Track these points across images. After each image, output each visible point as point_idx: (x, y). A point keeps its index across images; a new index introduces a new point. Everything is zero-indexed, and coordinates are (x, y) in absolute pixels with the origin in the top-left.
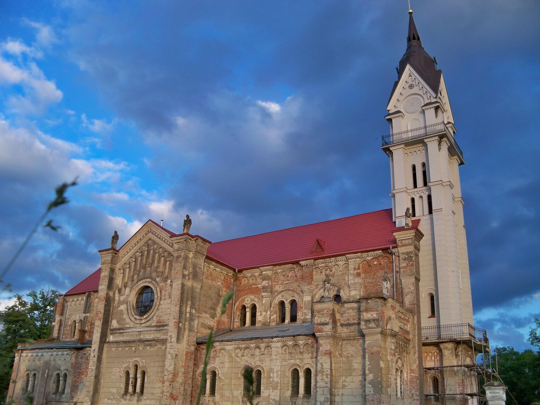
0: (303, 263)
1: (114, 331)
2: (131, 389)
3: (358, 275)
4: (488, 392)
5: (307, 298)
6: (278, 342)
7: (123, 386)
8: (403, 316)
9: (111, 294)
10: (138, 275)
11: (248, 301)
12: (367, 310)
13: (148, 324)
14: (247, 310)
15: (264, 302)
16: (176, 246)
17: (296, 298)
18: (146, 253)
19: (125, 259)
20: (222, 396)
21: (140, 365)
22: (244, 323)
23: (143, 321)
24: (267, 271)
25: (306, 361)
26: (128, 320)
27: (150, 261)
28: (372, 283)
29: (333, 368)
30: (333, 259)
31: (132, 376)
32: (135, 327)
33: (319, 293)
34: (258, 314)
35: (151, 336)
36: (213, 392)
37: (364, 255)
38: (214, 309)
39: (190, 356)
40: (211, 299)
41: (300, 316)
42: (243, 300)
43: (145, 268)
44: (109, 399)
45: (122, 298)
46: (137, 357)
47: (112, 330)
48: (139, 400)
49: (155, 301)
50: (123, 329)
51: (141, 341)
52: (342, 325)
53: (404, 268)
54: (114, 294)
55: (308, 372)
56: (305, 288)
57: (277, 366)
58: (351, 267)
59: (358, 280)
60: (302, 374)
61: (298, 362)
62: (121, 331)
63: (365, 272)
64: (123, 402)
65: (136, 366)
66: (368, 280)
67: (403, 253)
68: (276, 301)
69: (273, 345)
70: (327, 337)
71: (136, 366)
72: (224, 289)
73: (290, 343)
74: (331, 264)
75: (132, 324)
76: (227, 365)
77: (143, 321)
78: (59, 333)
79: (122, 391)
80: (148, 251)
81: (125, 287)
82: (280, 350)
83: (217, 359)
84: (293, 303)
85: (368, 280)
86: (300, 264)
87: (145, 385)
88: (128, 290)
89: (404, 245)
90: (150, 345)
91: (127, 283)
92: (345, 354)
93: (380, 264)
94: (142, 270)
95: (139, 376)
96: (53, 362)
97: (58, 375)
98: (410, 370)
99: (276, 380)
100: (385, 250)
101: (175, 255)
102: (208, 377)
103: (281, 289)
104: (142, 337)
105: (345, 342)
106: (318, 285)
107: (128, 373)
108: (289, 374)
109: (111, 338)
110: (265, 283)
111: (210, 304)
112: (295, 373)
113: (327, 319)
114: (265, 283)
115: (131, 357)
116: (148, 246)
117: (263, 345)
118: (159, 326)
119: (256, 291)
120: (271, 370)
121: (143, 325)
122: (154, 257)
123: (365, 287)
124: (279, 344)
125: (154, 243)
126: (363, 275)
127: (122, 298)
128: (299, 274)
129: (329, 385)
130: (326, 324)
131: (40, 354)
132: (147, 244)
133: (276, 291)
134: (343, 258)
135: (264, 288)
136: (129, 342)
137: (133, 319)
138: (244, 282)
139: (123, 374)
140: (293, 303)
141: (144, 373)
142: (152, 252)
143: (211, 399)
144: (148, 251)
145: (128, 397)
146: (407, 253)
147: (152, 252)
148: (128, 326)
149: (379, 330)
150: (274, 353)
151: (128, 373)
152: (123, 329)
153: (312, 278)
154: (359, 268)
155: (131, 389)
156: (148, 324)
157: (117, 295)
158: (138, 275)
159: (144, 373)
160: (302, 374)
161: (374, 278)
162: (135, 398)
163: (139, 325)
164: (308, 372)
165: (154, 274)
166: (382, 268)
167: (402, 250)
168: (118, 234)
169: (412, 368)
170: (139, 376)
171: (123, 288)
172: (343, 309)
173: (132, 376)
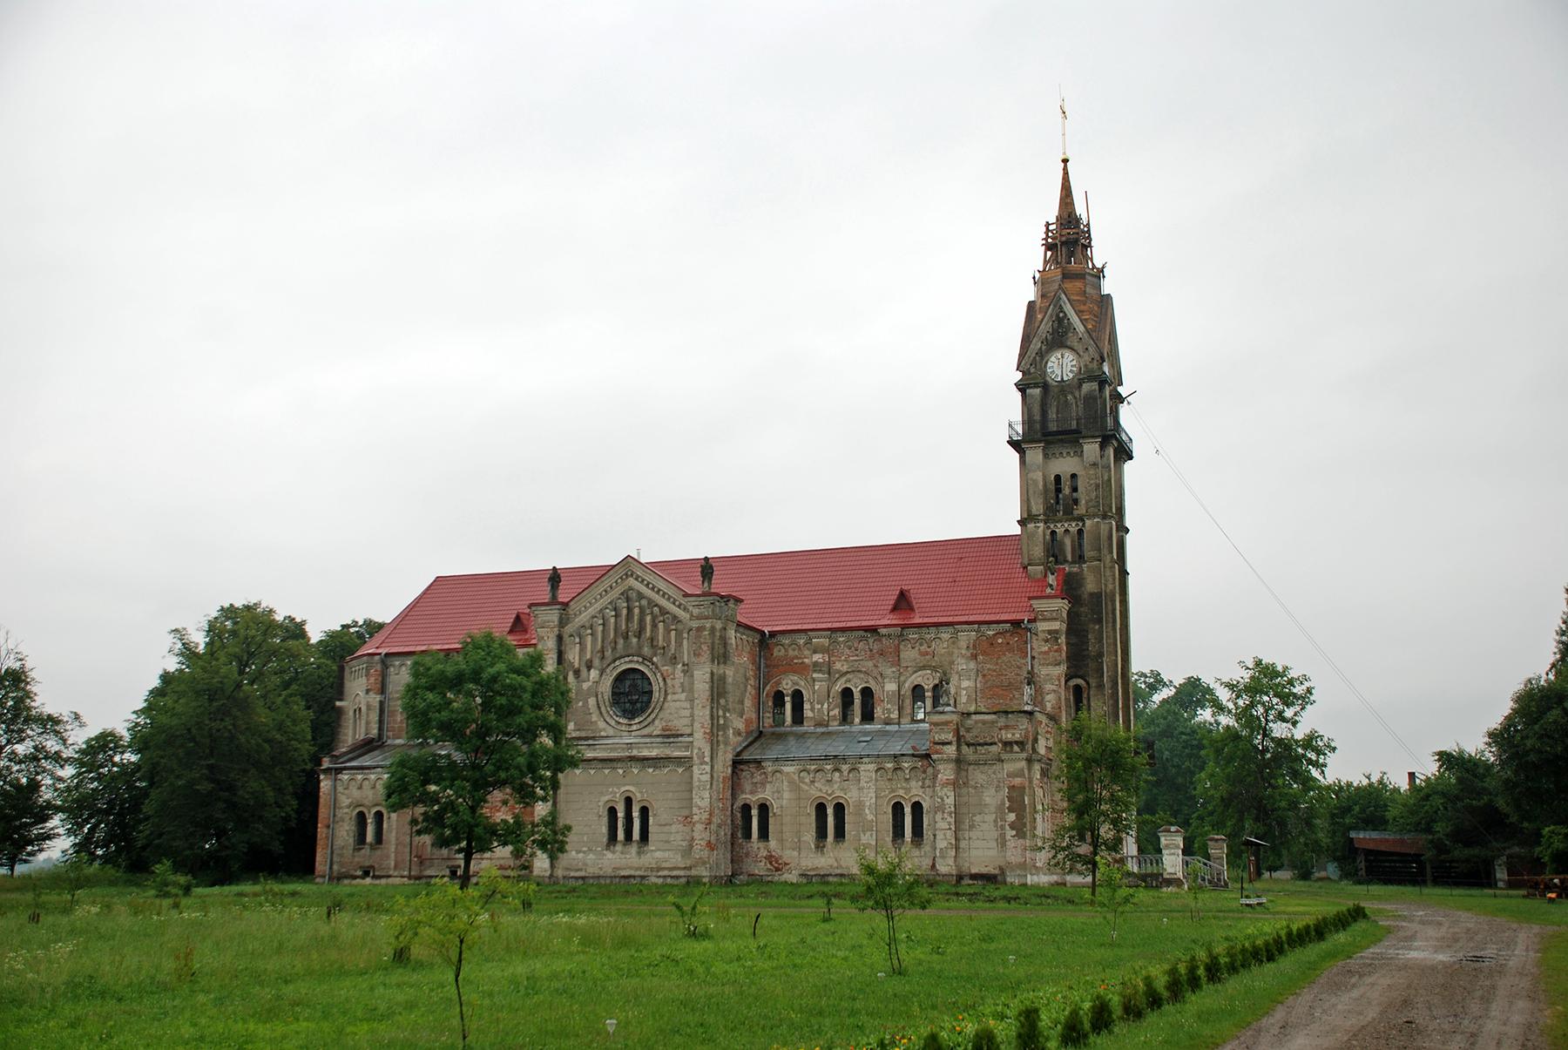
2: (621, 835)
3: (974, 657)
4: (1162, 839)
5: (891, 687)
7: (605, 830)
10: (614, 649)
11: (787, 685)
12: (1007, 727)
13: (645, 731)
14: (787, 699)
16: (696, 611)
17: (872, 685)
18: (625, 612)
19: (583, 618)
20: (781, 841)
25: (914, 792)
26: (601, 724)
27: (635, 625)
30: (933, 629)
31: (621, 815)
32: (616, 735)
34: (806, 706)
35: (654, 753)
36: (764, 834)
37: (983, 628)
38: (742, 702)
41: (878, 712)
42: (778, 683)
43: (626, 637)
45: (585, 686)
49: (656, 694)
50: (593, 738)
51: (632, 759)
52: (969, 745)
56: (889, 671)
57: (869, 798)
59: (972, 665)
60: (908, 810)
61: (901, 792)
63: (984, 653)
64: (609, 855)
65: (629, 802)
68: (839, 687)
69: (862, 767)
70: (948, 760)
71: (629, 802)
73: (890, 765)
75: (611, 732)
76: (786, 795)
78: (380, 729)
79: (605, 840)
80: (630, 609)
81: (589, 668)
84: (867, 693)
88: (594, 674)
89: (1045, 620)
90: (655, 767)
95: (636, 814)
99: (870, 817)
101: (695, 624)
103: (845, 669)
104: (635, 753)
107: (612, 812)
110: (817, 657)
112: (898, 809)
113: (950, 737)
114: (817, 657)
115: (619, 786)
117: (845, 768)
118: (668, 736)
119: (801, 669)
120: (860, 806)
122: (642, 621)
124: (872, 767)
125: (641, 596)
127: (585, 686)
128: (876, 647)
130: (950, 743)
132: (626, 596)
133: (838, 671)
134: (951, 629)
135: (816, 664)
136: (611, 760)
138: (778, 652)
141: (644, 812)
142: (636, 611)
143: (761, 845)
144: (630, 609)
145: (619, 847)
146: (1050, 632)
147: (636, 611)
149: (1024, 755)
151: (612, 812)
152: (593, 738)
155: (621, 835)
156: (645, 731)
159: (644, 812)
160: (908, 810)
162: (634, 849)
164: (917, 808)
165: (646, 650)
166: (1011, 650)
167: (1043, 626)
170: (636, 814)
171: (584, 670)
173: (621, 815)
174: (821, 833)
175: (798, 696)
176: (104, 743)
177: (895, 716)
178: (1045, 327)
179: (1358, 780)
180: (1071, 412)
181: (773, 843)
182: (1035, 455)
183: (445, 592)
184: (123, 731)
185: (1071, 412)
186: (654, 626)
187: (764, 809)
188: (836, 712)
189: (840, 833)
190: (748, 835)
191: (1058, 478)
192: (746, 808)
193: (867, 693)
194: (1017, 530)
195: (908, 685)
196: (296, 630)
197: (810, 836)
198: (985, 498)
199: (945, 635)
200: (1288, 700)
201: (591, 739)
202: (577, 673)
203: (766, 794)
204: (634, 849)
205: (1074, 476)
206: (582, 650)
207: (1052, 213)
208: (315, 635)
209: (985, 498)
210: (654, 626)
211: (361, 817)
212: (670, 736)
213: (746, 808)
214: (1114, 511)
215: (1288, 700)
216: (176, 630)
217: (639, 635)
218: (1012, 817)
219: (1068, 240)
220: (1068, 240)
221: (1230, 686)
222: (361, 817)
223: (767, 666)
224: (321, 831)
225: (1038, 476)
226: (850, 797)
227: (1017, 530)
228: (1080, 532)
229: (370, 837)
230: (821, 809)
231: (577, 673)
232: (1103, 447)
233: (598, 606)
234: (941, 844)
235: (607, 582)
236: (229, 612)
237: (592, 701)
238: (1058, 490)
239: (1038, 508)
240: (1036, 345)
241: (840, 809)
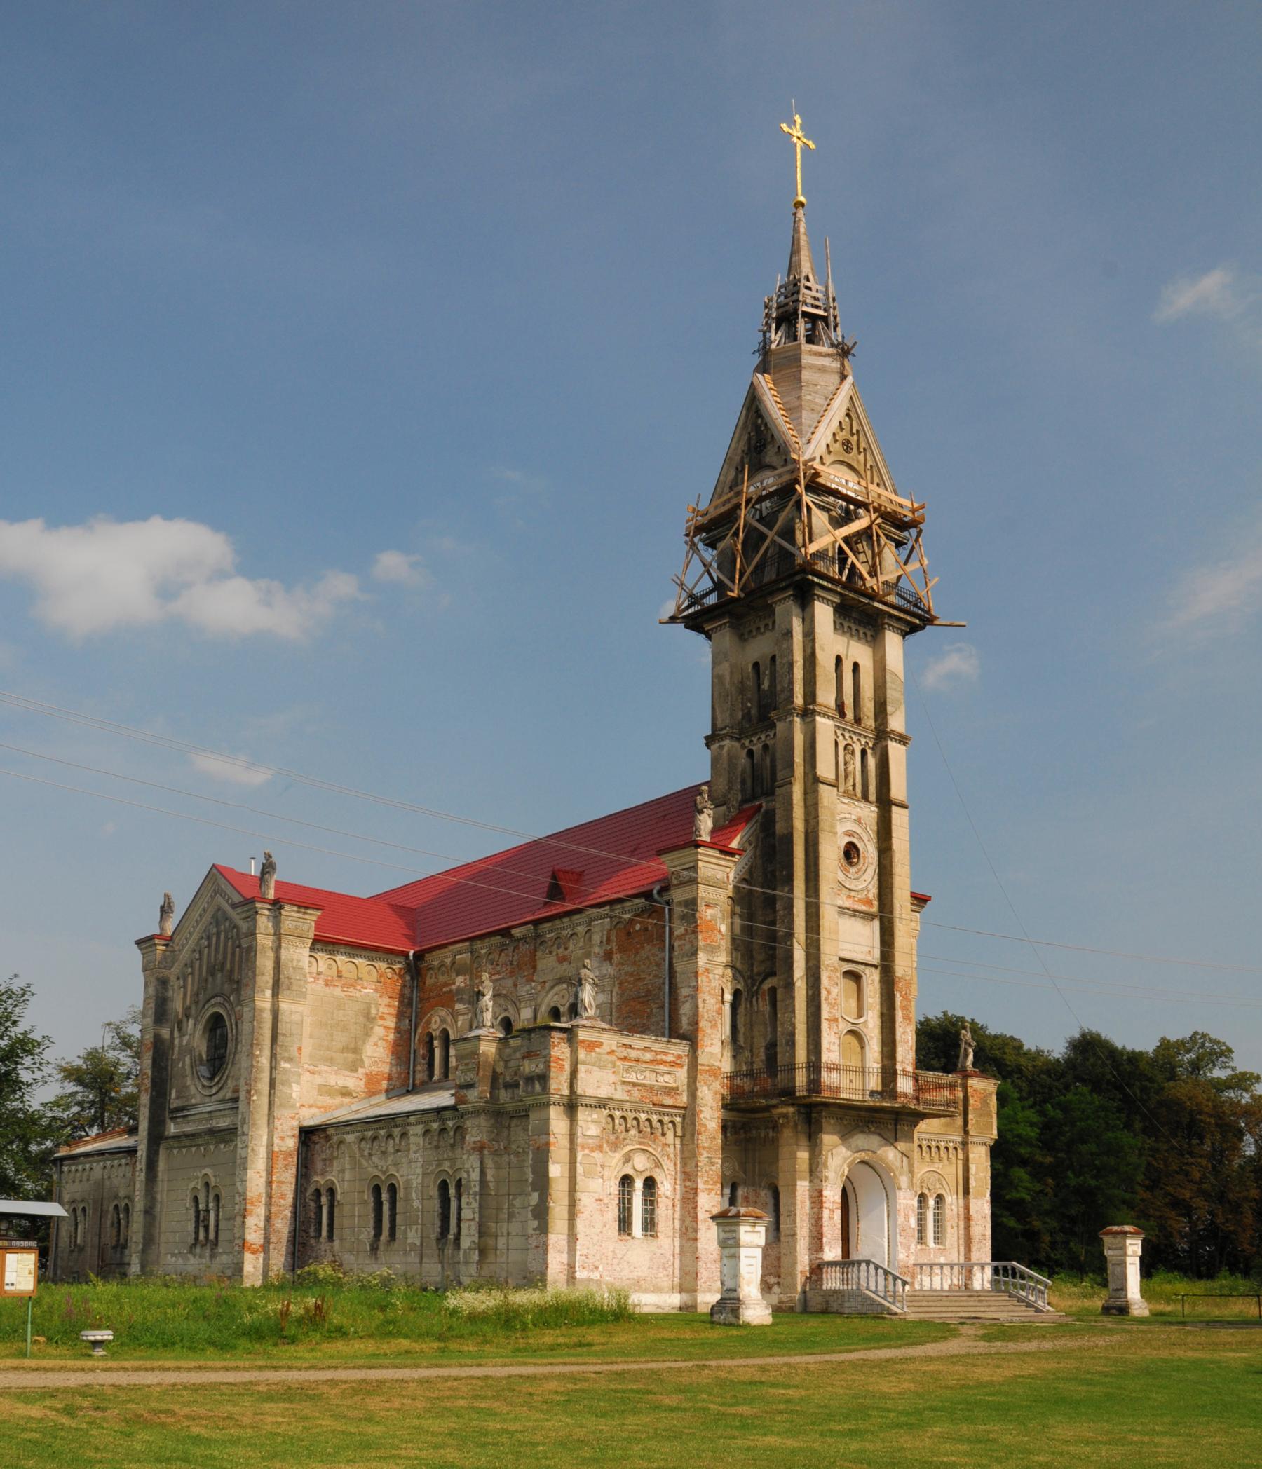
0: (517, 932)
1: (176, 1113)
3: (608, 956)
6: (418, 1123)
8: (648, 1056)
9: (165, 1033)
13: (220, 1096)
14: (436, 1043)
15: (459, 1023)
21: (213, 1182)
22: (431, 1074)
23: (214, 1090)
28: (631, 975)
29: (489, 1178)
33: (546, 1001)
39: (285, 1159)
40: (345, 1029)
44: (173, 1255)
46: (206, 1167)
47: (172, 1111)
53: (681, 937)
54: (172, 1033)
62: (186, 1113)
63: (622, 949)
64: (192, 1260)
66: (626, 968)
67: (680, 903)
72: (386, 1000)
73: (435, 1126)
74: (564, 933)
77: (214, 1090)
79: (191, 1240)
81: (188, 1016)
82: (421, 1141)
83: (335, 1163)
85: (626, 968)
86: (511, 936)
87: (221, 1227)
88: (191, 1022)
91: (189, 1008)
92: (513, 1147)
93: (646, 929)
94: (210, 979)
96: (107, 1183)
97: (116, 1207)
98: (684, 1172)
100: (648, 895)
102: (324, 1200)
105: (514, 1122)
106: (545, 982)
107: (196, 1199)
108: (434, 1192)
109: (172, 1129)
111: (341, 1039)
116: (218, 924)
117: (397, 1132)
120: (408, 1182)
121: (214, 1098)
123: (621, 984)
126: (617, 957)
129: (477, 1216)
131: (88, 1166)
137: (200, 1088)
139: (189, 1202)
148: (193, 1101)
150: (413, 1148)
151: (196, 1199)
153: (534, 968)
154: (608, 941)
156: (220, 1096)
157: (176, 1034)
158: (205, 989)
161: (635, 963)
163: (207, 1099)
168: (274, 859)
169: (688, 1170)
172: (508, 1051)
181: (337, 1243)
195: (544, 1009)
197: (367, 1233)
203: (332, 1177)
216: (109, 1024)
223: (421, 1000)
226: (401, 1177)
231: (180, 1023)
237: (187, 1060)
241: (393, 1189)
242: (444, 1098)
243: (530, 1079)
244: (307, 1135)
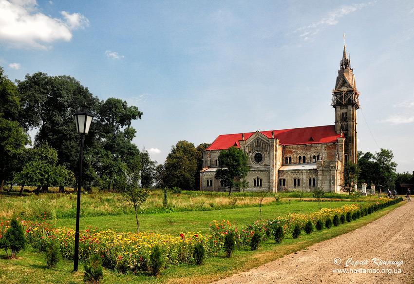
2: (256, 185)
5: (309, 156)
7: (253, 184)
11: (288, 155)
16: (271, 142)
17: (305, 156)
19: (248, 143)
20: (287, 186)
24: (295, 147)
26: (253, 164)
31: (256, 181)
32: (255, 166)
36: (284, 185)
48: (260, 188)
55: (314, 180)
56: (308, 153)
57: (305, 177)
58: (323, 147)
63: (328, 149)
65: (258, 178)
68: (298, 156)
88: (251, 154)
95: (259, 181)
107: (255, 180)
112: (310, 180)
119: (291, 153)
120: (303, 179)
125: (260, 139)
140: (304, 157)
151: (255, 180)
155: (256, 185)
162: (259, 187)
164: (314, 180)
170: (259, 181)
173: (256, 181)
174: (295, 184)
175: (290, 158)
176: (160, 167)
177: (309, 162)
178: (340, 82)
179: (402, 173)
180: (345, 99)
181: (286, 186)
182: (338, 109)
183: (221, 138)
184: (163, 164)
185: (345, 99)
186: (263, 145)
187: (284, 180)
188: (298, 161)
189: (299, 185)
190: (281, 185)
191: (343, 113)
192: (280, 180)
193: (304, 157)
194: (334, 124)
196: (192, 145)
197: (293, 185)
198: (327, 117)
199: (320, 145)
200: (388, 156)
201: (251, 167)
202: (248, 154)
203: (285, 177)
204: (259, 187)
205: (346, 113)
206: (249, 150)
207: (341, 58)
208: (196, 146)
209: (327, 117)
210: (263, 145)
211: (208, 181)
212: (266, 166)
213: (280, 180)
214: (354, 119)
215: (388, 156)
217: (260, 146)
218: (332, 181)
219: (345, 64)
220: (345, 64)
221: (378, 154)
222: (208, 181)
224: (200, 184)
225: (339, 113)
226: (301, 177)
227: (334, 124)
228: (347, 124)
229: (209, 185)
230: (295, 180)
232: (352, 107)
233: (250, 142)
234: (318, 186)
235: (253, 136)
236: (180, 142)
238: (343, 115)
239: (339, 119)
240: (339, 86)
241: (299, 180)
242: (315, 167)
243: (332, 167)
244: (279, 171)
